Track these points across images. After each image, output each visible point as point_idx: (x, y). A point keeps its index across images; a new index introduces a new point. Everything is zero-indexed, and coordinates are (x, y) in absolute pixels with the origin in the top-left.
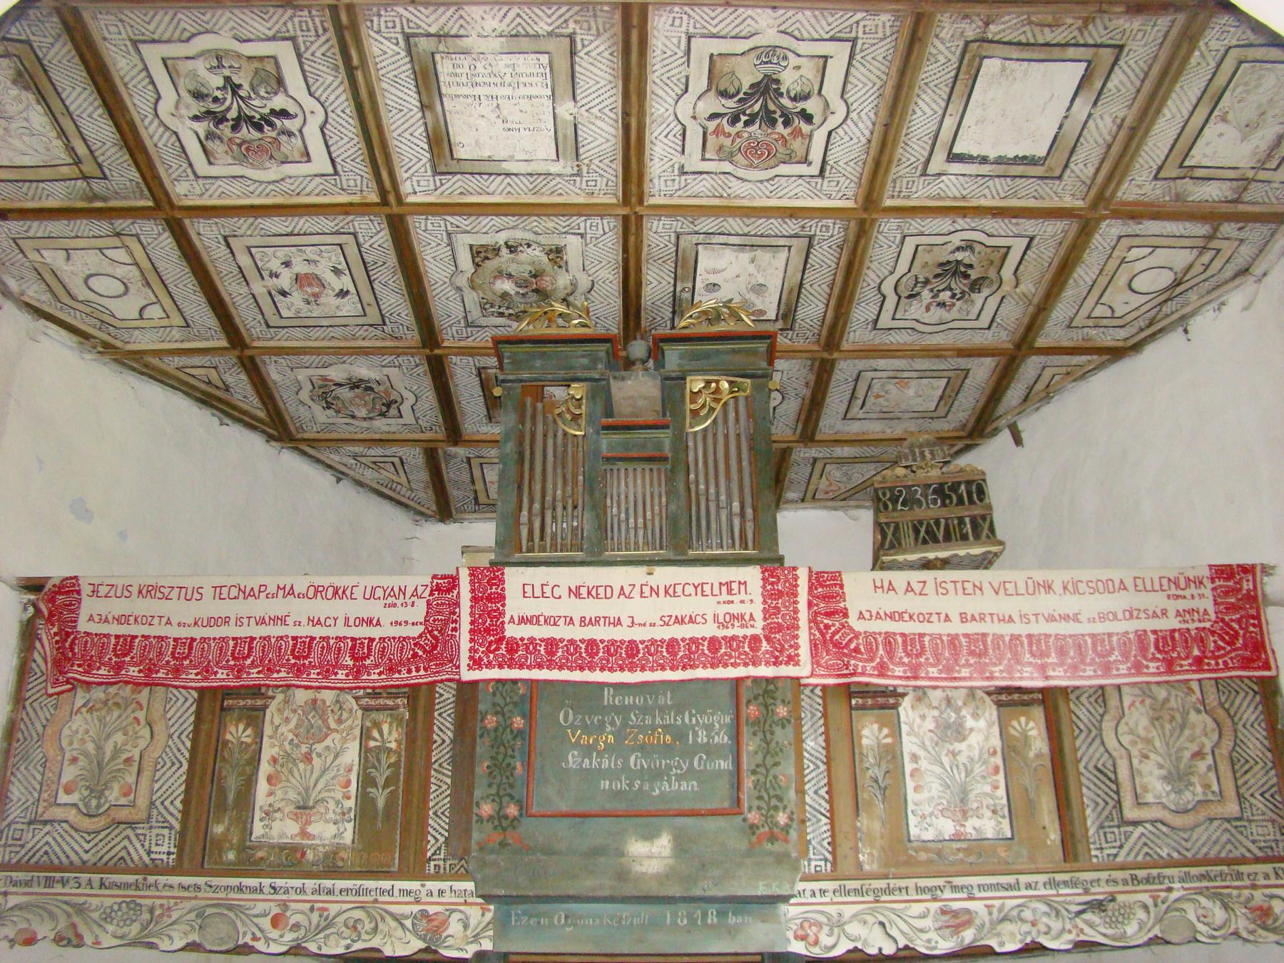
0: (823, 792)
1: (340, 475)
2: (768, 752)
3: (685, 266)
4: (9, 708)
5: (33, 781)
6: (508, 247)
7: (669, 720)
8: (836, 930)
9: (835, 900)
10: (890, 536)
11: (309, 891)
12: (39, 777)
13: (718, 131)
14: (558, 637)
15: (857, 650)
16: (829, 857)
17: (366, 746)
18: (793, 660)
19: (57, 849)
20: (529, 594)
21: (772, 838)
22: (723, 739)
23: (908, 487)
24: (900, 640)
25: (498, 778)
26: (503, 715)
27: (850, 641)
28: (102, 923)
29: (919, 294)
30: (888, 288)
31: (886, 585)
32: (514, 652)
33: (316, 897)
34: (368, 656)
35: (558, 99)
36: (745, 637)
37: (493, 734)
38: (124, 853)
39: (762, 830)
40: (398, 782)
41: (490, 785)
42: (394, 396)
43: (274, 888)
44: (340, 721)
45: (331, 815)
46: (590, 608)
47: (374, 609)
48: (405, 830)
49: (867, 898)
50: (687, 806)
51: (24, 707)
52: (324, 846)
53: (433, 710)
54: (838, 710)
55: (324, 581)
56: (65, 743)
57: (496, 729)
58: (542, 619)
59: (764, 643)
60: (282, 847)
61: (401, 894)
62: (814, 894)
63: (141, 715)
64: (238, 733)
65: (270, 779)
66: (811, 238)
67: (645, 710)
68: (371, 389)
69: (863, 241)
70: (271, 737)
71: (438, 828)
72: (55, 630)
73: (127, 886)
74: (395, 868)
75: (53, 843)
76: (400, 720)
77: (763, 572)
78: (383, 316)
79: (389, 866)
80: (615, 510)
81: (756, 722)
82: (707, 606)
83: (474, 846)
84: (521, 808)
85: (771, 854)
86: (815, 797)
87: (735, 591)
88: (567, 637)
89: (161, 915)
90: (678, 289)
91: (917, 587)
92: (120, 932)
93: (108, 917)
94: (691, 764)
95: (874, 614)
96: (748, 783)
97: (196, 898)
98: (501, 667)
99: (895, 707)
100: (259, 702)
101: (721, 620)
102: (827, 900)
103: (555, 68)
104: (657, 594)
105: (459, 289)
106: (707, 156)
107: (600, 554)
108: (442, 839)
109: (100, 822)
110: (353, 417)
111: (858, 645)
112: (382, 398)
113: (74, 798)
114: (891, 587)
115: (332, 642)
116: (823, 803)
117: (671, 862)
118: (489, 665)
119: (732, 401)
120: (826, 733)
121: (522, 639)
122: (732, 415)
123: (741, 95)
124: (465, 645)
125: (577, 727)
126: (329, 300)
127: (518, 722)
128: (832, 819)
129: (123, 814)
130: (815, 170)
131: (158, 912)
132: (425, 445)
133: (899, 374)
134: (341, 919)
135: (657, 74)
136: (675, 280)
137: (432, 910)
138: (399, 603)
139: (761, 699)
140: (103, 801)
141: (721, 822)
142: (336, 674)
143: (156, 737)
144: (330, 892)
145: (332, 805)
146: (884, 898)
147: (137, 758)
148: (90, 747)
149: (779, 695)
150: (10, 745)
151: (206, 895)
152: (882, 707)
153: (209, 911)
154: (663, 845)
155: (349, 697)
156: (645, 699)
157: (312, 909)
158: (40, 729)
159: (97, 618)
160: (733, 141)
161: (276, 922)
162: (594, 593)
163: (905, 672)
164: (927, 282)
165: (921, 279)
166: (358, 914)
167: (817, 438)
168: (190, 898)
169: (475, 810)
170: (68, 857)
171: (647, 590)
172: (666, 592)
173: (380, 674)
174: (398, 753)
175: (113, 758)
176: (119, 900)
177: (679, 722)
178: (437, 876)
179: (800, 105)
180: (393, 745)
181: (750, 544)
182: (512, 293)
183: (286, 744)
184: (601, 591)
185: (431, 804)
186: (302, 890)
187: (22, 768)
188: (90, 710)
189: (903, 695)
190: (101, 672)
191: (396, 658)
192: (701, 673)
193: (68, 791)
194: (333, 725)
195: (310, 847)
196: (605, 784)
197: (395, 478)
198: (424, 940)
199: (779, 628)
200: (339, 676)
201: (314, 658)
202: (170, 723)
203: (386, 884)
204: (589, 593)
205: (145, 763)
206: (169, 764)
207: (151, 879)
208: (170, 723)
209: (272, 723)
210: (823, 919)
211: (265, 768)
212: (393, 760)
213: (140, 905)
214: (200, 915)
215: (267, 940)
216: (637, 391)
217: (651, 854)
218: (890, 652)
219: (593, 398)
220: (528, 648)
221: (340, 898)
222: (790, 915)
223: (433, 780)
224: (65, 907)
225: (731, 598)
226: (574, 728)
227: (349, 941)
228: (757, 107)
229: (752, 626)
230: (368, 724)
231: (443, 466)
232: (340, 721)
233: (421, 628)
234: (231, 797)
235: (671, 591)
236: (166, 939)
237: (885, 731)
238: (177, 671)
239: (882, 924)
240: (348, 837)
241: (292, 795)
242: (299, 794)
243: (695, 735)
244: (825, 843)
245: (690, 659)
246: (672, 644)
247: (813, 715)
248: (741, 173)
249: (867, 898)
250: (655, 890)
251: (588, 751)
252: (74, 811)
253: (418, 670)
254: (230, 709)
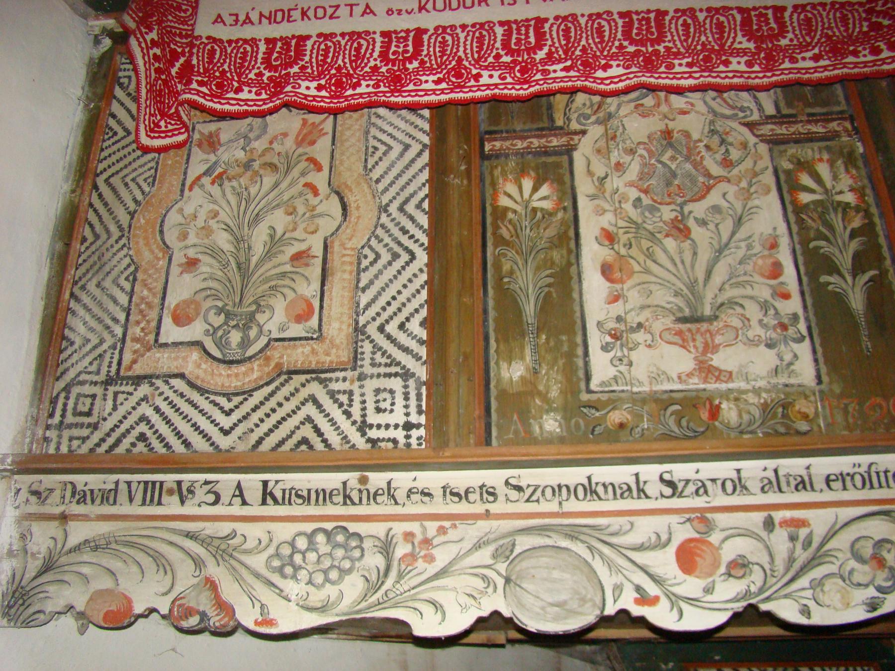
4: (67, 187)
5: (111, 306)
11: (754, 486)
12: (123, 299)
17: (794, 202)
19: (164, 429)
28: (276, 578)
33: (773, 498)
38: (307, 431)
40: (880, 259)
43: (671, 484)
45: (756, 331)
51: (95, 187)
52: (757, 392)
56: (171, 237)
60: (662, 402)
63: (320, 180)
64: (520, 195)
65: (606, 271)
70: (593, 197)
72: (154, 35)
73: (324, 496)
75: (155, 418)
89: (412, 557)
92: (317, 597)
93: (287, 564)
97: (487, 515)
100: (555, 142)
109: (255, 372)
113: (196, 331)
115: (701, 16)
129: (299, 355)
131: (402, 549)
134: (842, 541)
140: (253, 333)
142: (726, 63)
143: (353, 213)
144: (802, 484)
145: (753, 312)
147: (318, 250)
148: (223, 240)
150: (68, 245)
151: (511, 508)
153: (524, 543)
157: (769, 524)
158: (124, 219)
159: (229, 20)
161: (688, 558)
168: (476, 517)
170: (187, 444)
173: (816, 58)
175: (269, 255)
176: (309, 527)
180: (849, 198)
183: (628, 207)
186: (739, 485)
187: (92, 286)
188: (219, 179)
190: (243, 95)
193: (180, 320)
195: (725, 395)
201: (673, 40)
202: (381, 187)
205: (335, 260)
206: (386, 257)
207: (377, 479)
208: (381, 187)
209: (590, 173)
211: (592, 254)
213: (357, 535)
214: (505, 552)
215: (675, 600)
221: (828, 496)
224: (189, 544)
227: (871, 592)
230: (786, 165)
232: (727, 163)
234: (530, 309)
236: (428, 609)
238: (396, 82)
240: (805, 370)
241: (662, 297)
242: (677, 294)
252: (195, 355)
254: (497, 155)
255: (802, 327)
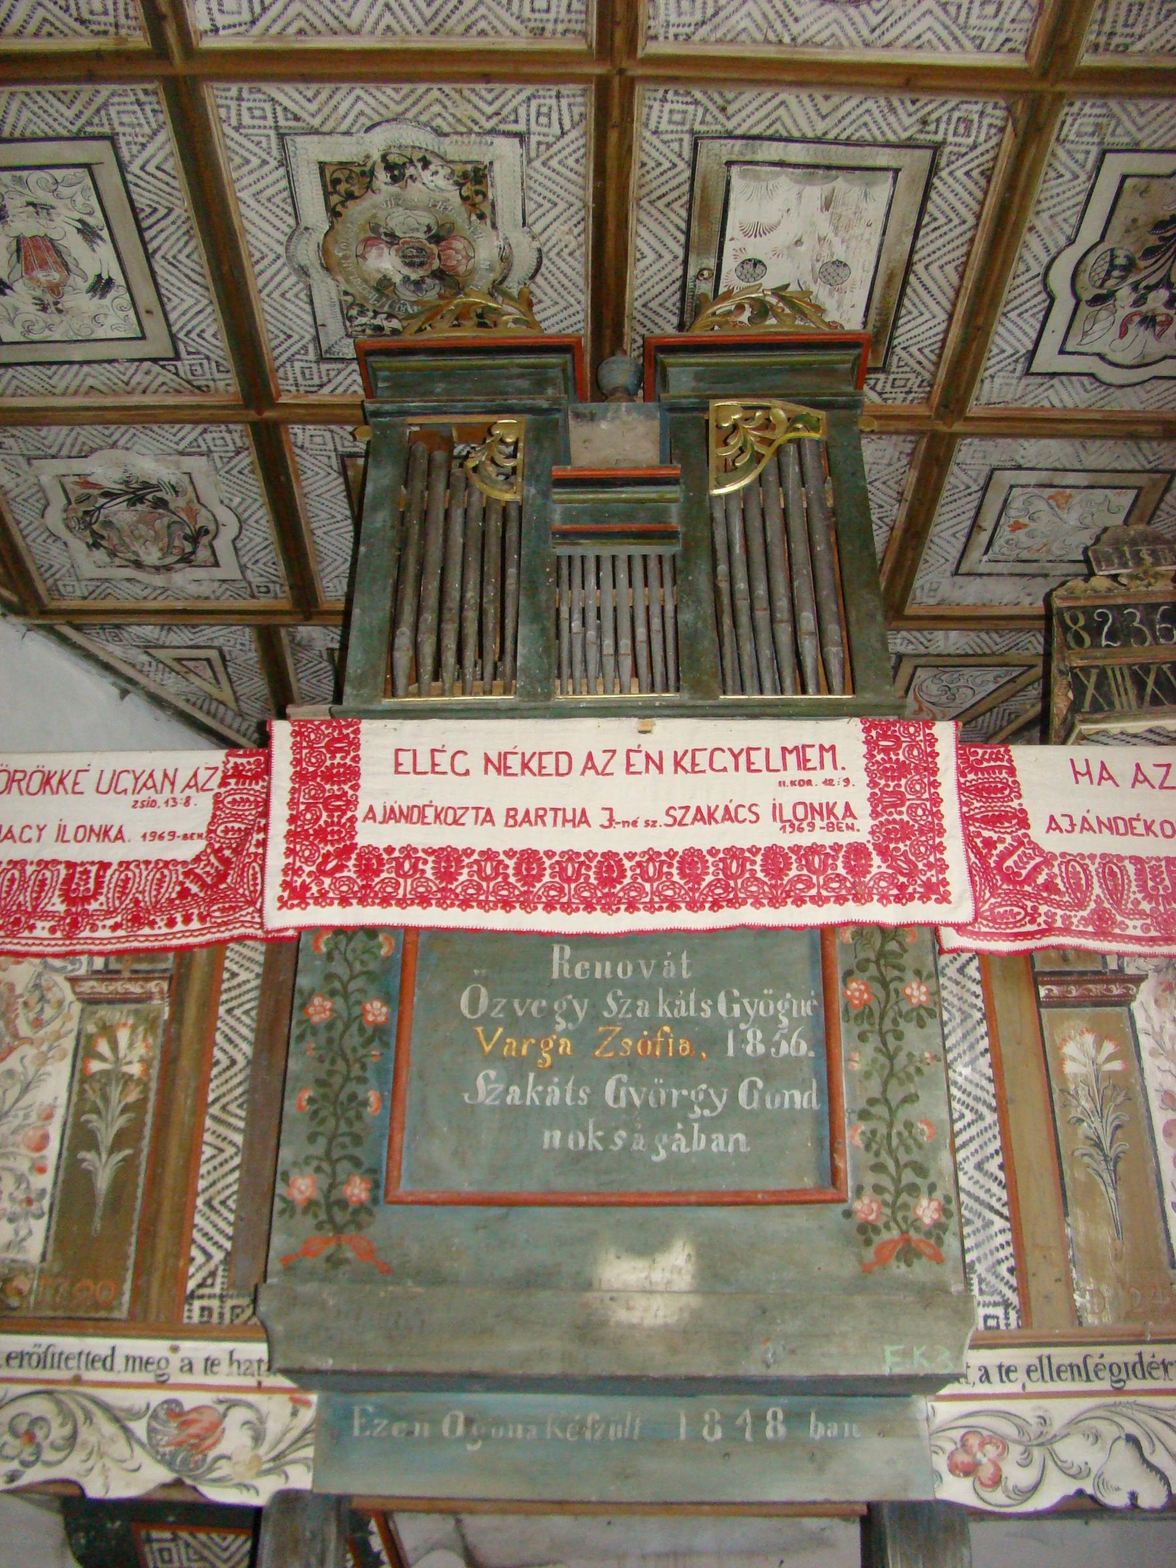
0: (993, 1166)
1: (127, 685)
2: (892, 1074)
3: (706, 218)
6: (389, 167)
7: (685, 1008)
8: (1037, 1453)
9: (1031, 1387)
10: (1091, 691)
14: (460, 848)
15: (1049, 886)
16: (1014, 1298)
17: (84, 1070)
18: (936, 891)
20: (407, 766)
21: (908, 1252)
22: (797, 1046)
23: (1119, 608)
24: (1131, 869)
25: (331, 1122)
26: (346, 996)
27: (1036, 869)
29: (1112, 294)
30: (1060, 280)
31: (1096, 771)
32: (372, 873)
34: (95, 896)
36: (837, 847)
37: (323, 1036)
39: (885, 1236)
40: (140, 1137)
41: (312, 1138)
42: (203, 520)
44: (38, 1023)
46: (527, 792)
47: (114, 811)
48: (148, 1234)
49: (1096, 1385)
50: (725, 1184)
53: (217, 1004)
54: (1014, 1005)
55: (28, 762)
57: (330, 1026)
58: (430, 812)
59: (876, 860)
61: (128, 1365)
62: (986, 1376)
66: (936, 148)
67: (636, 989)
68: (161, 503)
69: (1032, 151)
71: (212, 1232)
74: (122, 1313)
76: (152, 1025)
77: (867, 730)
78: (173, 338)
79: (109, 1307)
80: (576, 625)
81: (865, 1014)
82: (760, 790)
83: (275, 1265)
84: (376, 1185)
85: (906, 1285)
86: (978, 1175)
87: (814, 762)
88: (480, 846)
90: (692, 272)
91: (1156, 775)
94: (734, 1097)
95: (1078, 821)
96: (853, 1136)
98: (344, 901)
99: (1124, 1001)
101: (787, 815)
102: (1015, 1388)
104: (660, 768)
105: (303, 271)
107: (549, 695)
108: (218, 1256)
110: (138, 565)
111: (1052, 876)
112: (182, 523)
114: (1105, 774)
115: (29, 869)
116: (995, 1188)
117: (694, 1301)
118: (322, 899)
119: (792, 449)
120: (994, 1051)
121: (390, 850)
122: (793, 470)
124: (276, 858)
125: (497, 1022)
126: (80, 300)
127: (377, 1011)
128: (1015, 1222)
132: (259, 620)
133: (1058, 479)
136: (687, 248)
137: (189, 1399)
138: (160, 799)
139: (873, 969)
141: (799, 1218)
142: (32, 928)
146: (1133, 1384)
149: (907, 960)
152: (1099, 1002)
154: (676, 1265)
155: (60, 979)
156: (637, 969)
162: (534, 765)
163: (1146, 928)
164: (1130, 267)
165: (1120, 261)
166: (40, 1406)
167: (909, 611)
169: (280, 1189)
171: (638, 760)
172: (677, 764)
174: (143, 1083)
177: (707, 1013)
178: (204, 1331)
180: (135, 1069)
181: (836, 682)
182: (397, 279)
184: (548, 761)
185: (202, 1184)
189: (1138, 980)
191: (147, 900)
192: (748, 915)
194: (24, 1029)
196: (553, 1138)
197: (215, 692)
198: (170, 1464)
199: (904, 832)
200: (38, 933)
203: (99, 1345)
204: (525, 765)
210: (1009, 1430)
212: (133, 1096)
216: (621, 437)
217: (650, 1286)
218: (1116, 893)
219: (537, 440)
220: (400, 866)
222: (938, 1421)
223: (207, 1137)
225: (805, 775)
226: (488, 1022)
227: (15, 1465)
229: (851, 828)
230: (91, 1028)
231: (290, 661)
232: (38, 1023)
233: (199, 846)
235: (686, 763)
237: (1109, 1048)
239: (1132, 1440)
240: (34, 1249)
243: (741, 1039)
244: (1003, 1269)
245: (726, 888)
246: (691, 861)
247: (966, 1017)
249: (1096, 1385)
250: (661, 1363)
251: (516, 1070)
253: (187, 919)
255: (46, 1203)
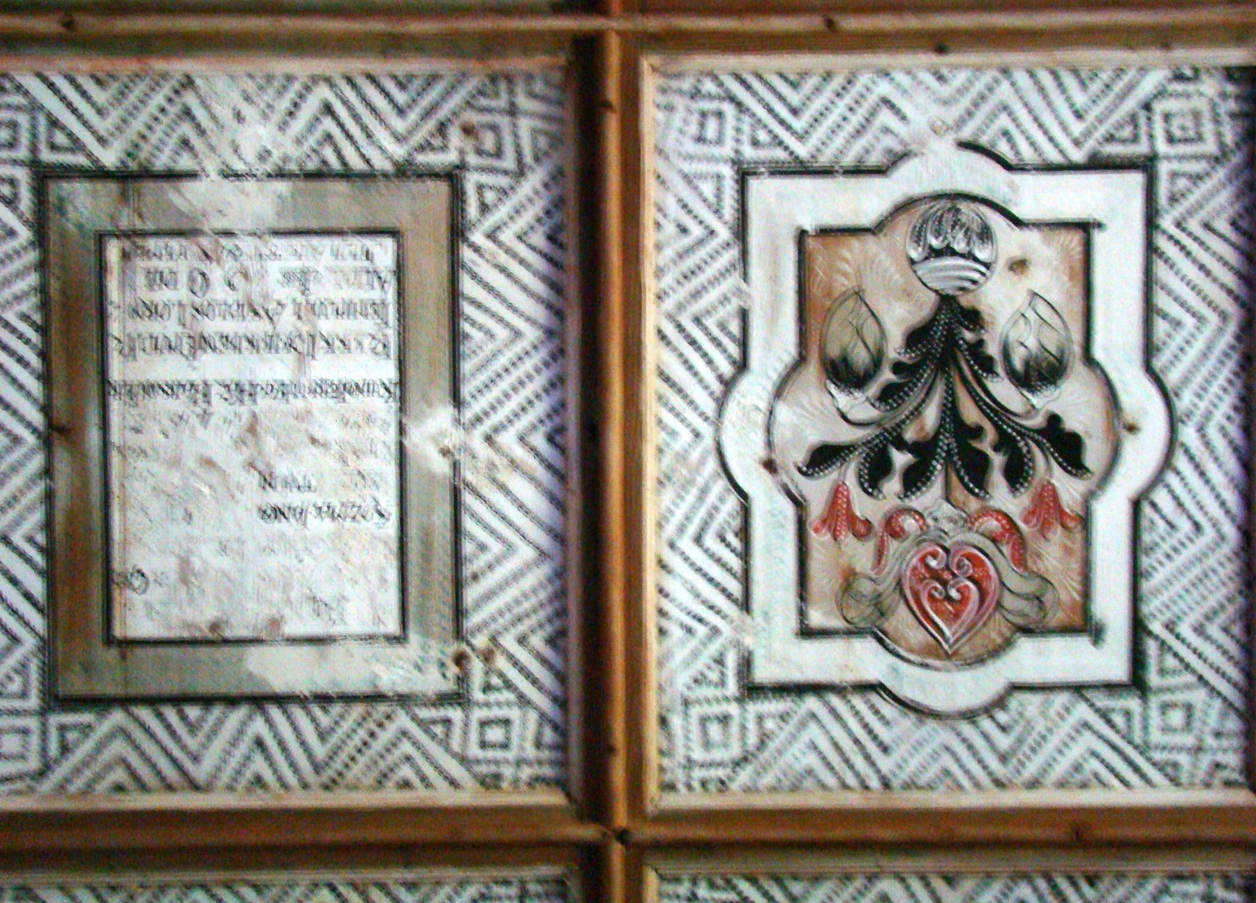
13: (839, 515)
35: (413, 397)
103: (411, 277)
106: (816, 618)
123: (887, 376)
130: (1110, 661)
135: (669, 304)
160: (880, 553)
179: (1046, 401)
228: (931, 415)
248: (917, 683)
